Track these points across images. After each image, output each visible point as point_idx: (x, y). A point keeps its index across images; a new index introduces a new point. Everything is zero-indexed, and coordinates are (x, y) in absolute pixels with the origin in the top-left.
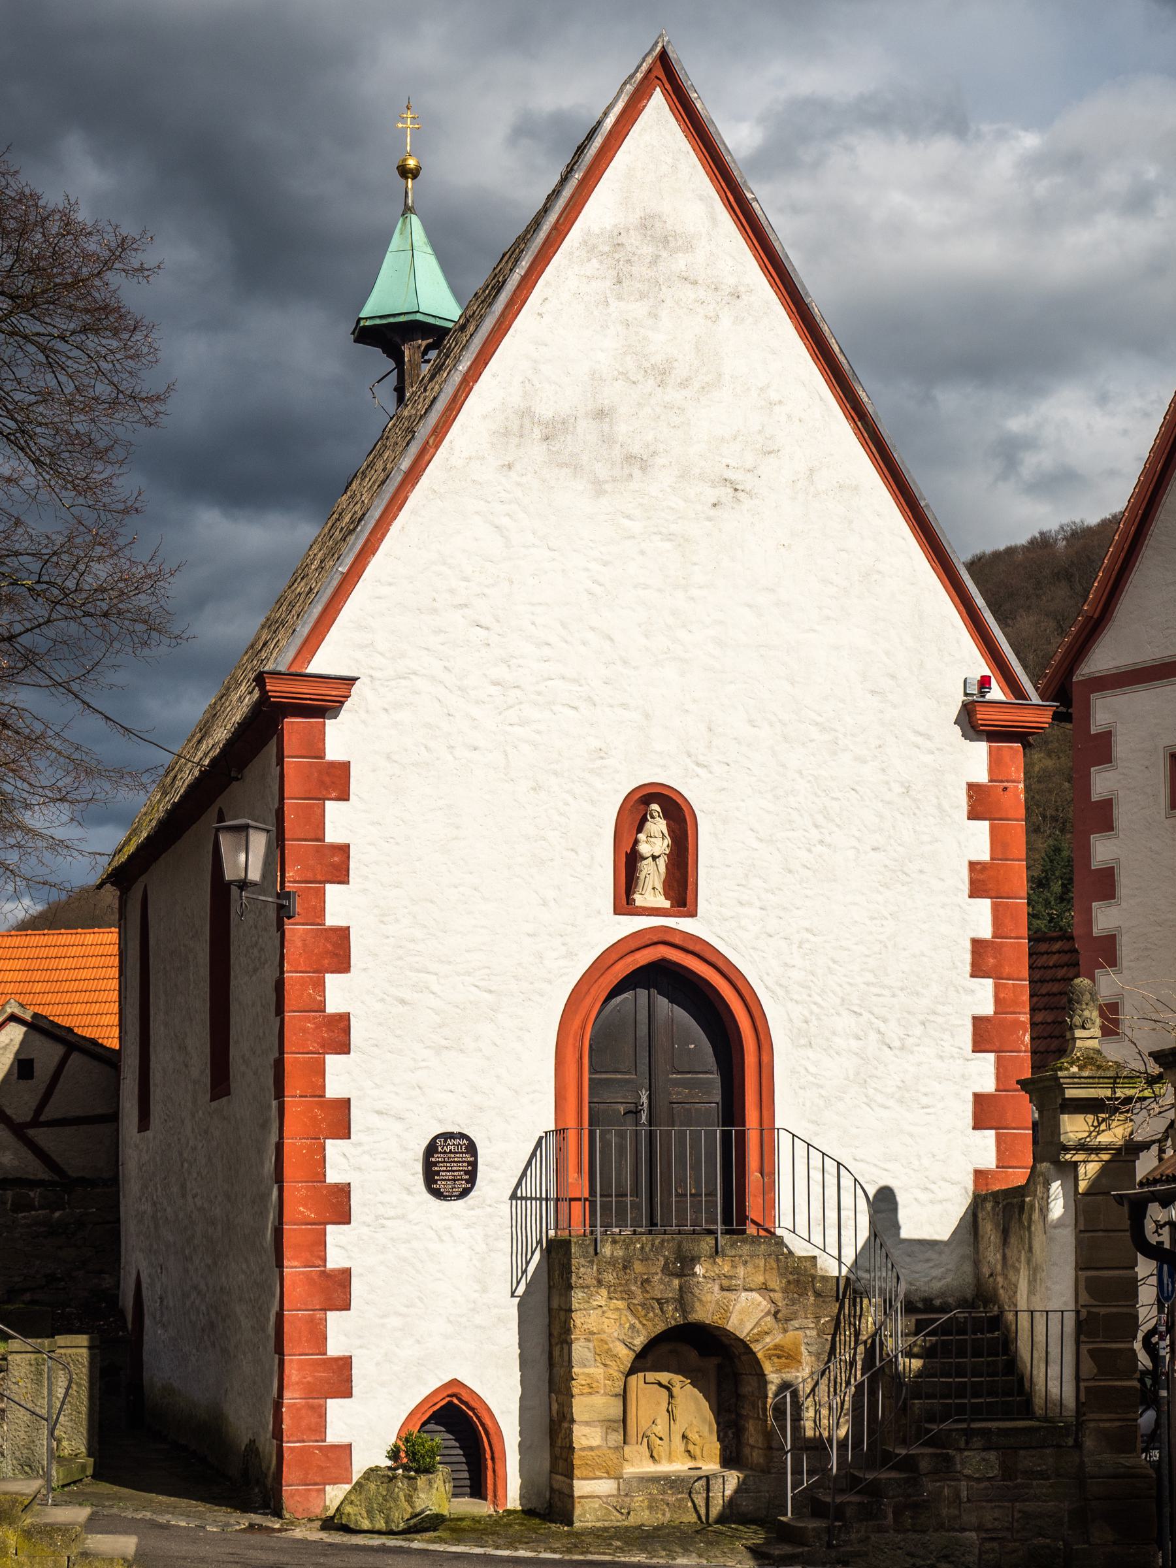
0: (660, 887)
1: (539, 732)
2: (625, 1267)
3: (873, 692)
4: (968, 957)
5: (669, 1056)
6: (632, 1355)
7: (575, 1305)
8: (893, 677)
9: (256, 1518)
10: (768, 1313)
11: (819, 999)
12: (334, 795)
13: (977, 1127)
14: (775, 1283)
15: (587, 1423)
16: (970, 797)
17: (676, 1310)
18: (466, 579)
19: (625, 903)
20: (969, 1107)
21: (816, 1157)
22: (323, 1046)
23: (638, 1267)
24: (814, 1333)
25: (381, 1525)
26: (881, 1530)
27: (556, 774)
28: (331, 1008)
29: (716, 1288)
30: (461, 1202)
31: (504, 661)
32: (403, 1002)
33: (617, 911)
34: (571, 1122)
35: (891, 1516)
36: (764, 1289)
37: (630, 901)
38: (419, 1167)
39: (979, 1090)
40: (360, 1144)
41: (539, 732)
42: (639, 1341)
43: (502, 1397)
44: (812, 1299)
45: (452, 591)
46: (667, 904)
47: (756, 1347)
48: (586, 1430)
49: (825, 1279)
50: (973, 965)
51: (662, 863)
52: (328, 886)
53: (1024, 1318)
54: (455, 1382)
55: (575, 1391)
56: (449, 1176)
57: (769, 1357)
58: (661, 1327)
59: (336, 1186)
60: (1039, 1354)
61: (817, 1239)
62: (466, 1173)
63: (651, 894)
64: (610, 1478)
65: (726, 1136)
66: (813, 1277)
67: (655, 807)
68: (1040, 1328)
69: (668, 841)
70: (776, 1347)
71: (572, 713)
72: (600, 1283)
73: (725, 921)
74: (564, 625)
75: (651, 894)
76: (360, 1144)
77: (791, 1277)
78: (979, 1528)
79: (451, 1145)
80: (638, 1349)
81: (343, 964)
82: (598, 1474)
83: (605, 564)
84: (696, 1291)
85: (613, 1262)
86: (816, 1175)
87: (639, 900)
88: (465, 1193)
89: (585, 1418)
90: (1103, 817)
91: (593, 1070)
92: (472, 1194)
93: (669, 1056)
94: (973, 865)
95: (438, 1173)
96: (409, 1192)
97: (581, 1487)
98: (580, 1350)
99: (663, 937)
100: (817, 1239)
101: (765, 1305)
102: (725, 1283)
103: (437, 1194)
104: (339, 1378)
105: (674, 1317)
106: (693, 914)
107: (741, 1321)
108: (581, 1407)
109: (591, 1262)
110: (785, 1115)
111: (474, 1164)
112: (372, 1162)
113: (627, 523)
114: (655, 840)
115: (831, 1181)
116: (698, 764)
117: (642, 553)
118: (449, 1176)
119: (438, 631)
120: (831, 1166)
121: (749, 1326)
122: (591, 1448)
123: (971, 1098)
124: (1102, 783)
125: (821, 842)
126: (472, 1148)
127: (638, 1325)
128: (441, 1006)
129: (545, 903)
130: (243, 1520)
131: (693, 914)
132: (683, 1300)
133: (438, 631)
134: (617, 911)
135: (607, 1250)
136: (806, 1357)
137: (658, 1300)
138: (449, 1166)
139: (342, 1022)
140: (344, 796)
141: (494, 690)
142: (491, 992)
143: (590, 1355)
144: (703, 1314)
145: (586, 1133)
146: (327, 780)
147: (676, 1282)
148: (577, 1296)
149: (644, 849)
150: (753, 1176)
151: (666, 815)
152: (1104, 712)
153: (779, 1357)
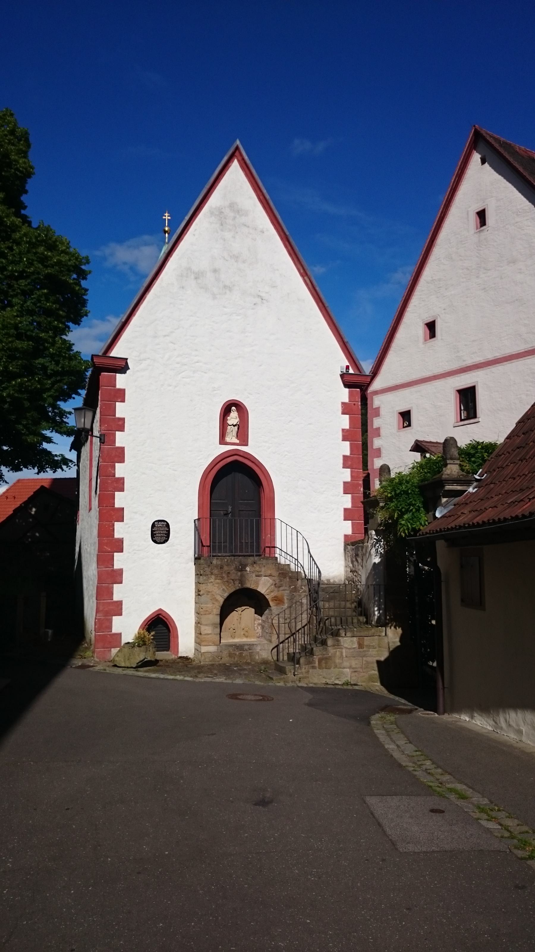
2: (221, 568)
4: (341, 461)
10: (272, 585)
12: (119, 400)
14: (276, 574)
15: (206, 625)
16: (342, 407)
17: (239, 583)
19: (222, 441)
21: (289, 529)
22: (114, 489)
23: (226, 568)
24: (288, 592)
26: (314, 668)
28: (117, 476)
29: (254, 575)
33: (220, 443)
35: (317, 662)
36: (270, 576)
40: (127, 524)
42: (226, 595)
44: (288, 580)
48: (207, 627)
52: (117, 432)
54: (160, 610)
56: (159, 535)
57: (272, 600)
59: (118, 539)
62: (166, 534)
63: (231, 437)
64: (215, 645)
67: (233, 408)
70: (275, 597)
72: (212, 574)
73: (257, 448)
75: (231, 437)
77: (280, 572)
78: (350, 667)
80: (225, 597)
82: (211, 644)
85: (217, 566)
86: (289, 536)
87: (228, 439)
92: (168, 542)
94: (343, 430)
95: (155, 534)
99: (236, 453)
102: (257, 573)
103: (155, 542)
105: (238, 586)
109: (209, 566)
110: (279, 514)
112: (132, 531)
118: (159, 535)
120: (294, 532)
122: (208, 634)
123: (343, 510)
126: (168, 525)
127: (225, 589)
135: (215, 562)
136: (286, 601)
137: (233, 580)
138: (160, 532)
139: (121, 481)
140: (123, 401)
144: (250, 584)
147: (239, 573)
151: (238, 411)
153: (276, 600)
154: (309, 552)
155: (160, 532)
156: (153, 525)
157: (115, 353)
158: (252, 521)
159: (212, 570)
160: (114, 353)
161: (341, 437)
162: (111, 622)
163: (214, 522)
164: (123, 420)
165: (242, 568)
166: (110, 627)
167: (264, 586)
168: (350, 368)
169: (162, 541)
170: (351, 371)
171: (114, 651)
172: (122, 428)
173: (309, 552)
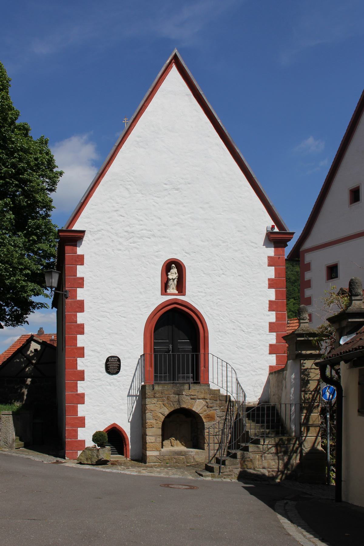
0: (175, 287)
1: (139, 245)
3: (239, 231)
4: (268, 305)
5: (177, 335)
6: (164, 417)
7: (147, 403)
8: (245, 227)
9: (59, 459)
11: (222, 318)
13: (270, 353)
18: (117, 203)
20: (268, 348)
25: (90, 463)
27: (144, 256)
28: (78, 322)
29: (189, 399)
30: (116, 375)
31: (129, 225)
32: (99, 320)
33: (162, 294)
34: (148, 352)
36: (204, 399)
37: (166, 291)
38: (104, 366)
39: (271, 343)
40: (87, 359)
41: (139, 245)
42: (167, 412)
43: (126, 428)
45: (113, 207)
46: (177, 292)
47: (201, 415)
48: (151, 437)
49: (223, 396)
50: (269, 307)
51: (176, 281)
53: (283, 406)
55: (147, 427)
57: (205, 418)
58: (172, 409)
60: (288, 417)
61: (220, 385)
63: (172, 289)
65: (193, 356)
66: (219, 396)
67: (173, 265)
68: (288, 409)
69: (177, 275)
70: (207, 415)
71: (148, 239)
72: (154, 397)
73: (195, 296)
74: (146, 215)
75: (172, 289)
76: (87, 359)
79: (113, 359)
80: (166, 415)
81: (82, 310)
83: (158, 197)
84: (184, 400)
87: (168, 291)
88: (117, 373)
89: (150, 434)
90: (308, 284)
91: (155, 339)
93: (177, 335)
96: (101, 373)
97: (149, 453)
98: (148, 415)
99: (176, 302)
100: (220, 385)
101: (204, 403)
102: (192, 397)
104: (81, 422)
105: (177, 407)
106: (184, 295)
107: (197, 408)
108: (149, 431)
111: (120, 365)
112: (91, 364)
113: (165, 186)
114: (173, 274)
115: (224, 369)
116: (186, 253)
117: (169, 194)
119: (109, 218)
120: (224, 364)
121: (199, 409)
122: (152, 443)
123: (268, 345)
124: (308, 276)
125: (223, 274)
126: (119, 360)
128: (111, 321)
129: (141, 293)
130: (54, 459)
131: (184, 295)
132: (179, 402)
133: (109, 218)
134: (162, 294)
139: (82, 326)
140: (82, 264)
141: (126, 234)
142: (125, 317)
143: (151, 417)
145: (153, 356)
146: (78, 260)
147: (177, 396)
148: (148, 400)
149: (170, 277)
150: (202, 368)
152: (308, 258)
154: (237, 380)
155: (113, 366)
156: (108, 360)
157: (77, 227)
158: (188, 356)
159: (155, 393)
160: (75, 228)
161: (267, 286)
162: (76, 432)
163: (156, 356)
164: (82, 279)
165: (179, 394)
166: (76, 436)
167: (198, 407)
168: (275, 227)
169: (115, 372)
170: (276, 230)
171: (79, 452)
172: (81, 285)
173: (237, 380)
